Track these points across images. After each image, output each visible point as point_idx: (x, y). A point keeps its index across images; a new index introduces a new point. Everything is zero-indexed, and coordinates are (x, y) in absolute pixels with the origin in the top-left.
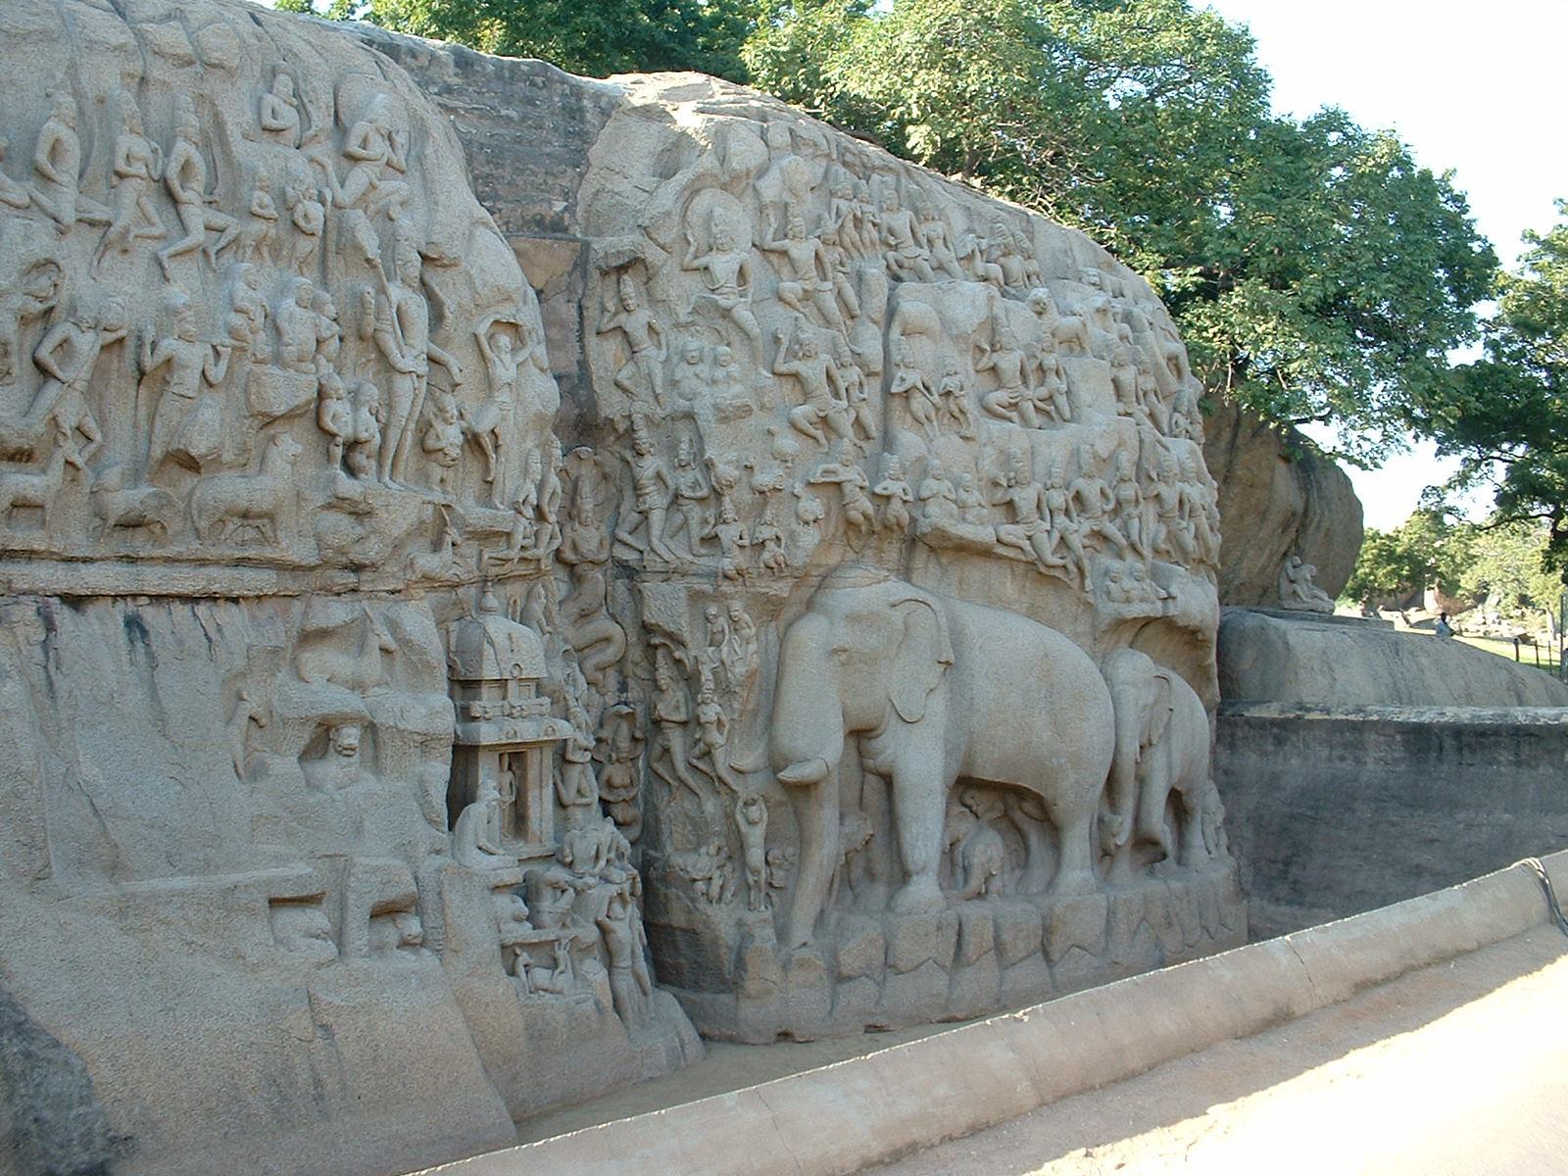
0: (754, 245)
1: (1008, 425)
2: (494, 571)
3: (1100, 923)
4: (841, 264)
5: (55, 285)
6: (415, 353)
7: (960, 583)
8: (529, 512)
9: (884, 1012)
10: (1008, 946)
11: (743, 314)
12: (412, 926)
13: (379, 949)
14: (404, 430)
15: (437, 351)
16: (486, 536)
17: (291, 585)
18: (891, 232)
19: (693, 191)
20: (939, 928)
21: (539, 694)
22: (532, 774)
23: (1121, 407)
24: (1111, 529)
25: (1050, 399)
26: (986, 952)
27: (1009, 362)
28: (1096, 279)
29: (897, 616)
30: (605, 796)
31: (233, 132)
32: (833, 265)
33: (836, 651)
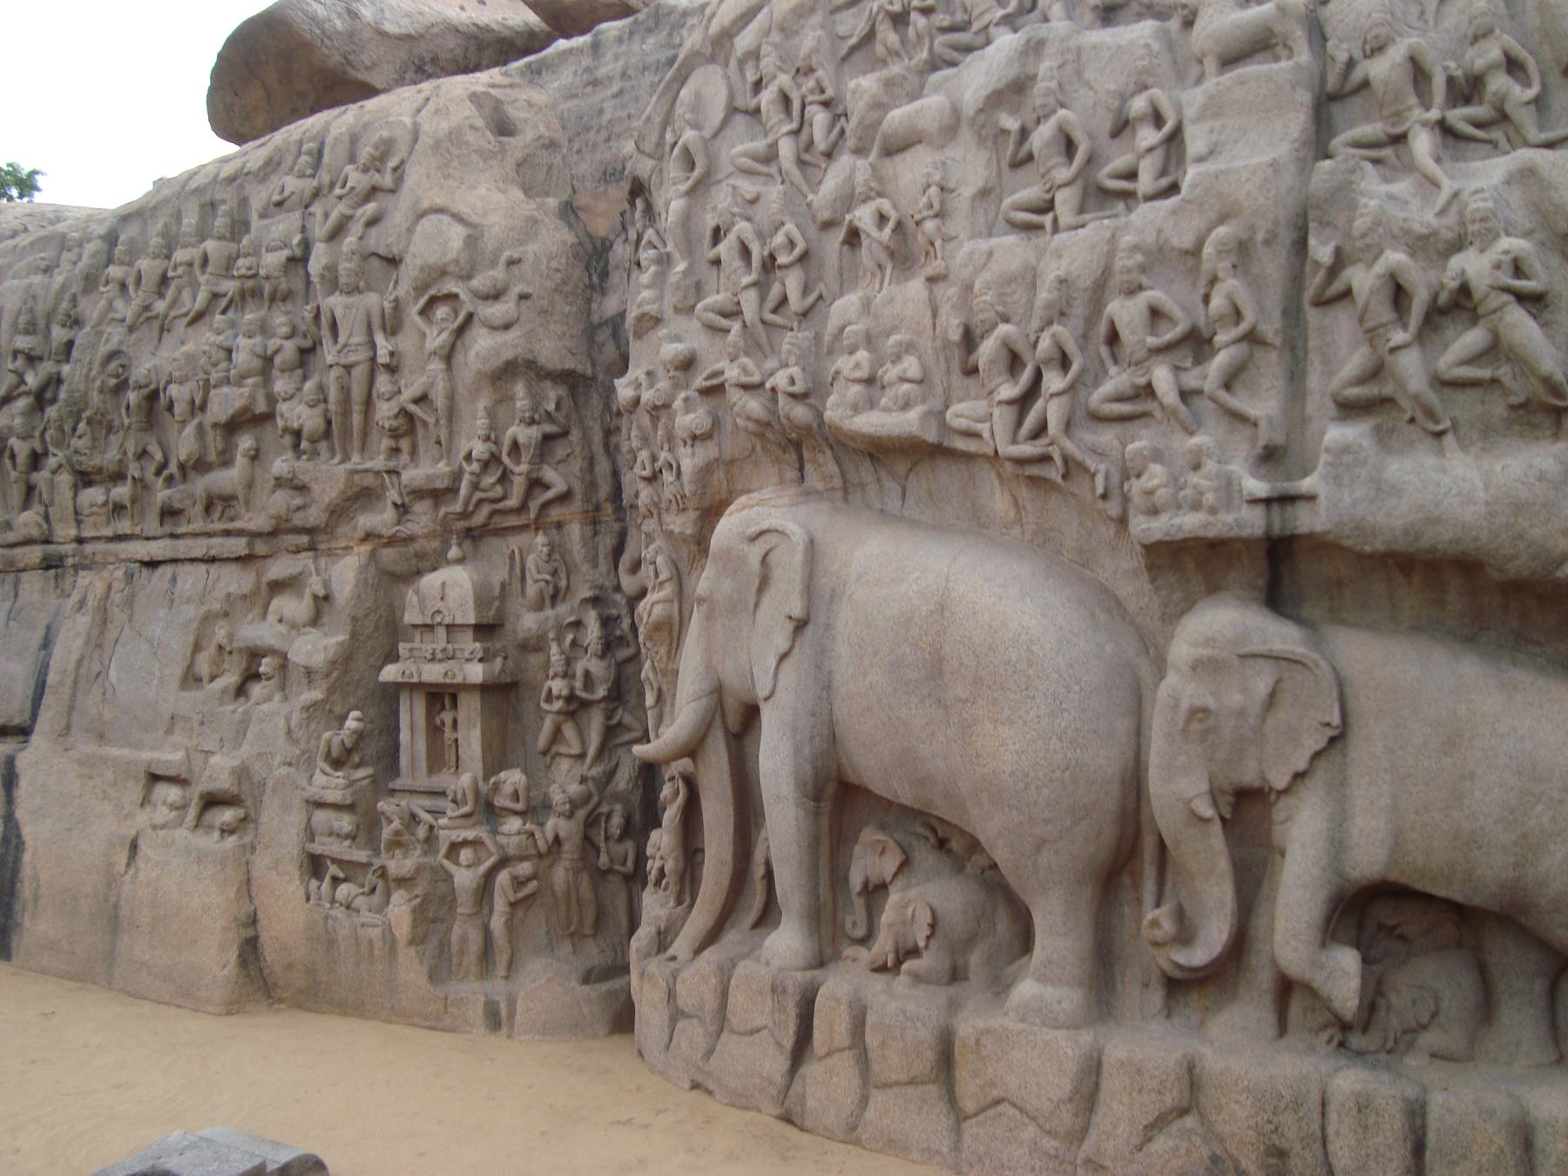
0: (732, 110)
2: (461, 525)
5: (122, 366)
6: (338, 347)
7: (930, 493)
8: (475, 467)
9: (709, 1074)
10: (872, 1054)
12: (228, 815)
13: (211, 827)
14: (346, 413)
15: (380, 339)
16: (437, 495)
17: (261, 548)
20: (773, 990)
21: (475, 640)
22: (462, 715)
26: (842, 1050)
29: (755, 553)
31: (254, 217)
33: (701, 601)
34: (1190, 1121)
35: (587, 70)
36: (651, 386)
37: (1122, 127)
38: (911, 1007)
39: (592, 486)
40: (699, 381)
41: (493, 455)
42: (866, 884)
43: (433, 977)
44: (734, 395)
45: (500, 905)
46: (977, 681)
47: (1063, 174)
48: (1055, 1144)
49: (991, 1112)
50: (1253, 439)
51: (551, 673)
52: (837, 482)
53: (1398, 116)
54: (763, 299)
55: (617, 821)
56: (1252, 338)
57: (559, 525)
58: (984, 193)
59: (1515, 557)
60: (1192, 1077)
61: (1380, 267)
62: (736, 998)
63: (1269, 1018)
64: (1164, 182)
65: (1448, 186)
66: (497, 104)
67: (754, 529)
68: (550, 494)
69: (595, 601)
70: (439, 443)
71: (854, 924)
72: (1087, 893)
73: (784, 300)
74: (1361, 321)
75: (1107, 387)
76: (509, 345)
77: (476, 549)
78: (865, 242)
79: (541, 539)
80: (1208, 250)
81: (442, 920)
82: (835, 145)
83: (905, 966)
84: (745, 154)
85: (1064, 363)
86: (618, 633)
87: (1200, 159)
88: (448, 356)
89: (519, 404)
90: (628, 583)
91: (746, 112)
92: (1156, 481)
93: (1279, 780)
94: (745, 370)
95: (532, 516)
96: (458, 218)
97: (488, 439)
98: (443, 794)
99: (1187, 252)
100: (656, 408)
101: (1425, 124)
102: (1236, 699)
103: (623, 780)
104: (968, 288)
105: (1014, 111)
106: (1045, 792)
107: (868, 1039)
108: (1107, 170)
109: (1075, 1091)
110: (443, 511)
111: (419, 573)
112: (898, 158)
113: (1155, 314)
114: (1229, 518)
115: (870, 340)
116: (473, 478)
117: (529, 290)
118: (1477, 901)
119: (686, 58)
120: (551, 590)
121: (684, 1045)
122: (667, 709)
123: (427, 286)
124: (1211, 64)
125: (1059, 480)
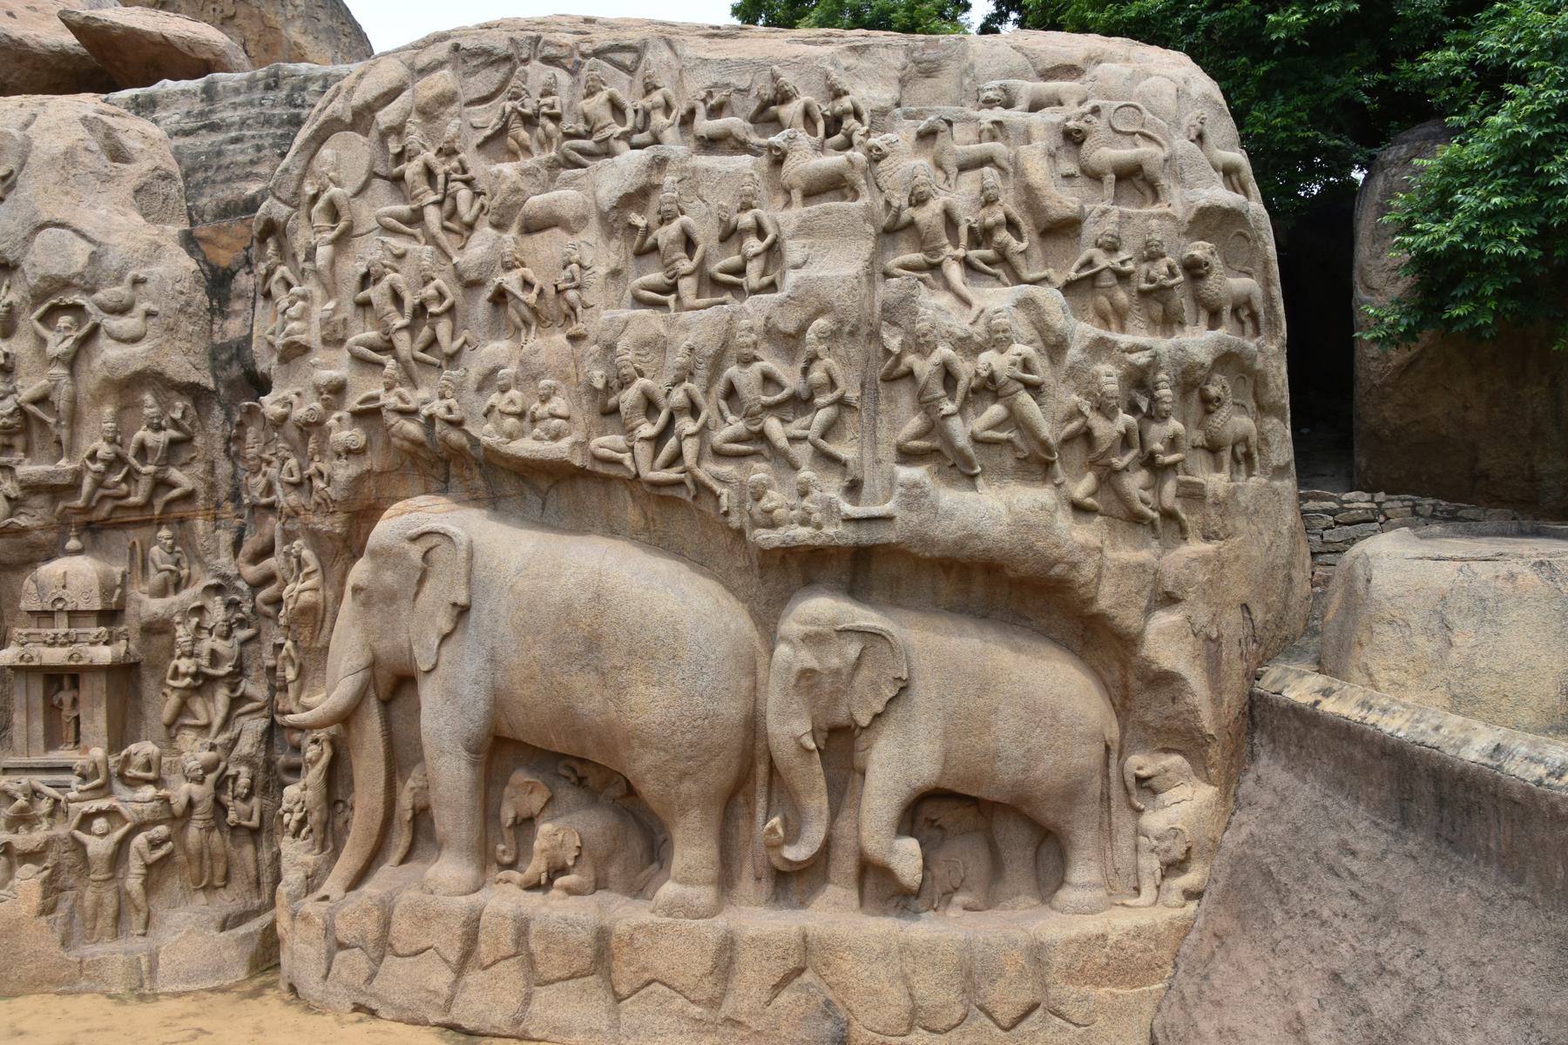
1: (625, 313)
3: (701, 962)
4: (465, 171)
9: (374, 995)
10: (538, 959)
11: (324, 252)
16: (54, 491)
18: (587, 120)
19: (320, 138)
22: (84, 694)
23: (917, 257)
24: (773, 426)
25: (740, 271)
27: (666, 234)
28: (991, 94)
29: (415, 552)
30: (278, 718)
32: (447, 174)
33: (356, 590)
34: (807, 977)
35: (202, 114)
36: (300, 406)
37: (730, 234)
38: (571, 914)
39: (212, 487)
40: (353, 403)
41: (117, 455)
42: (515, 819)
43: (65, 943)
44: (393, 419)
45: (135, 867)
46: (631, 653)
47: (686, 265)
48: (699, 1010)
49: (643, 992)
50: (844, 475)
51: (178, 652)
52: (481, 494)
53: (936, 251)
54: (413, 340)
55: (243, 781)
56: (842, 403)
57: (182, 521)
58: (615, 274)
59: (1026, 561)
60: (805, 943)
61: (936, 357)
62: (401, 926)
63: (855, 895)
64: (766, 280)
65: (978, 303)
66: (109, 133)
67: (415, 531)
68: (175, 492)
69: (217, 589)
70: (59, 442)
71: (504, 852)
72: (716, 812)
73: (433, 342)
74: (921, 394)
75: (727, 431)
76: (135, 357)
77: (94, 541)
78: (511, 302)
79: (164, 533)
80: (810, 335)
81: (71, 888)
82: (477, 217)
83: (558, 882)
84: (390, 216)
85: (694, 410)
86: (240, 615)
87: (796, 267)
88: (72, 362)
89: (147, 411)
90: (251, 572)
91: (385, 178)
92: (774, 504)
93: (864, 720)
94: (401, 397)
95: (157, 512)
96: (84, 236)
97: (112, 441)
98: (67, 769)
99: (790, 335)
100: (308, 424)
101: (955, 259)
102: (835, 662)
103: (246, 746)
104: (610, 347)
105: (641, 211)
106: (689, 736)
107: (532, 946)
108: (718, 265)
109: (715, 966)
110: (60, 506)
111: (30, 563)
112: (537, 236)
113: (768, 379)
114: (829, 530)
115: (517, 382)
116: (98, 477)
117: (154, 308)
118: (997, 798)
119: (326, 122)
120: (174, 578)
121: (345, 974)
122: (308, 681)
123: (46, 295)
124: (797, 195)
125: (689, 499)
